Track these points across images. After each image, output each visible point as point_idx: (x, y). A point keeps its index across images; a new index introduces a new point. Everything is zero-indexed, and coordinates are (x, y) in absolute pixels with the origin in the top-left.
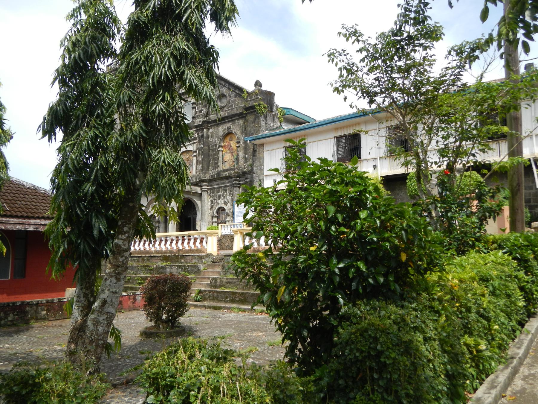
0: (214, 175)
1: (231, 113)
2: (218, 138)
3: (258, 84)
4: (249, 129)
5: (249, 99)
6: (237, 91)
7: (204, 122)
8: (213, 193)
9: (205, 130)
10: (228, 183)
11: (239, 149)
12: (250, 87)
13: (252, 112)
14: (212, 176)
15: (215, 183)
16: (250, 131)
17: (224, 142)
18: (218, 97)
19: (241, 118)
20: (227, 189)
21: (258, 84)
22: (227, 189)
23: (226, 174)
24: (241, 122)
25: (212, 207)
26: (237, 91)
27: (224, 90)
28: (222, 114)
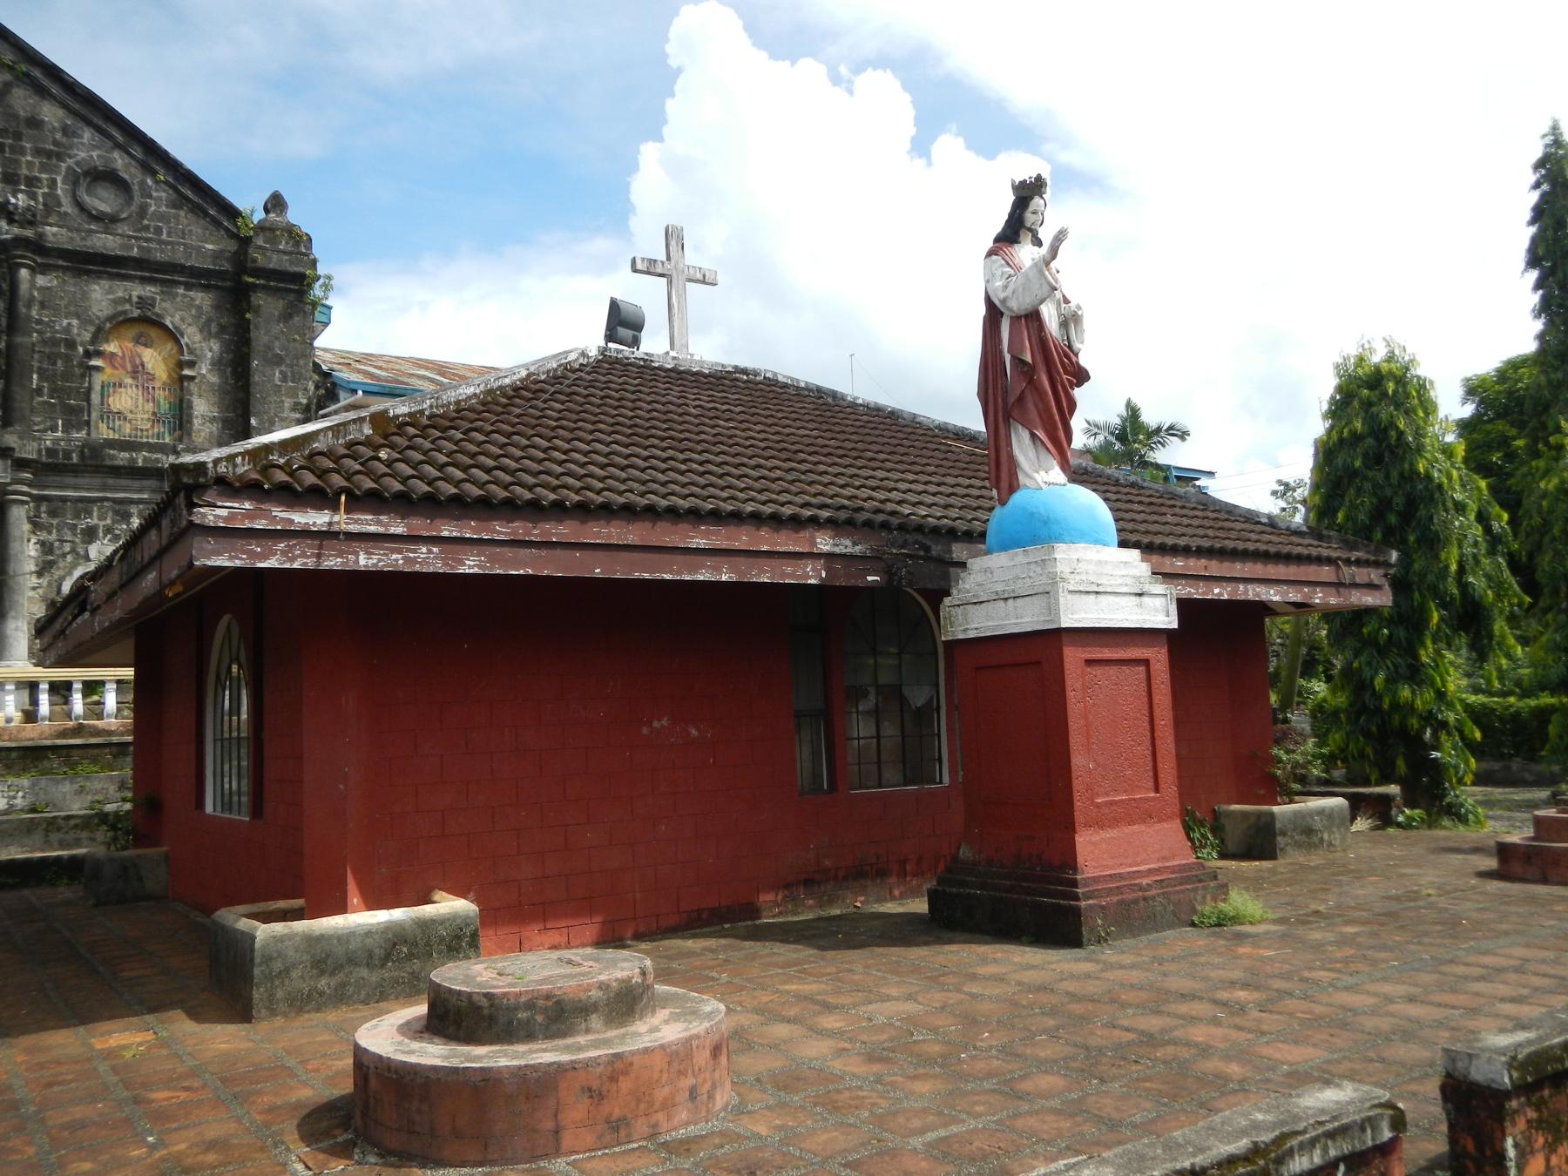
0: (67, 454)
1: (159, 256)
2: (85, 321)
3: (276, 203)
4: (260, 338)
5: (260, 242)
6: (189, 194)
7: (19, 242)
8: (53, 513)
9: (24, 272)
10: (140, 491)
11: (193, 387)
12: (250, 202)
13: (278, 290)
14: (51, 452)
15: (70, 480)
16: (269, 348)
17: (107, 341)
18: (87, 173)
19: (206, 288)
20: (134, 510)
21: (276, 203)
22: (134, 510)
23: (134, 460)
24: (202, 299)
25: (44, 568)
26: (189, 194)
27: (119, 161)
28: (105, 242)
